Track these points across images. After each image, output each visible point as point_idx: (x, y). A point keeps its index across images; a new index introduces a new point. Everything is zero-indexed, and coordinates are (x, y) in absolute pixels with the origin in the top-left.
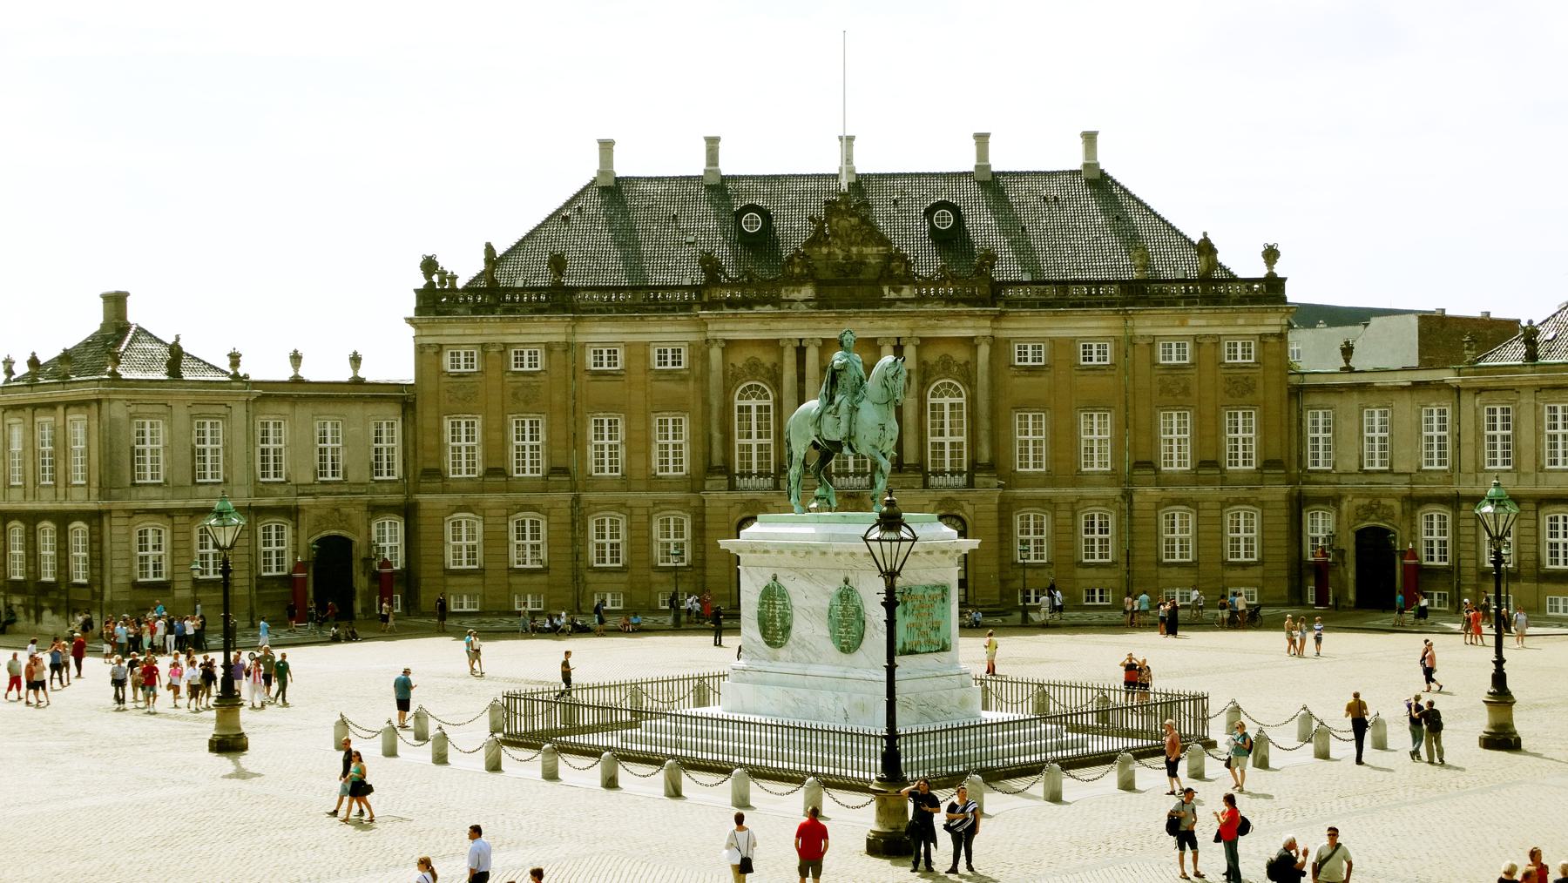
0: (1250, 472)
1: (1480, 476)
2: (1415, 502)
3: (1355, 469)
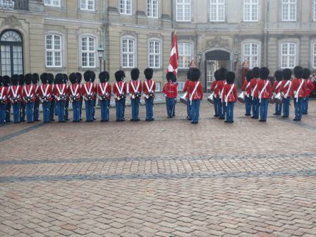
0: (156, 19)
1: (280, 24)
2: (240, 38)
3: (206, 21)
